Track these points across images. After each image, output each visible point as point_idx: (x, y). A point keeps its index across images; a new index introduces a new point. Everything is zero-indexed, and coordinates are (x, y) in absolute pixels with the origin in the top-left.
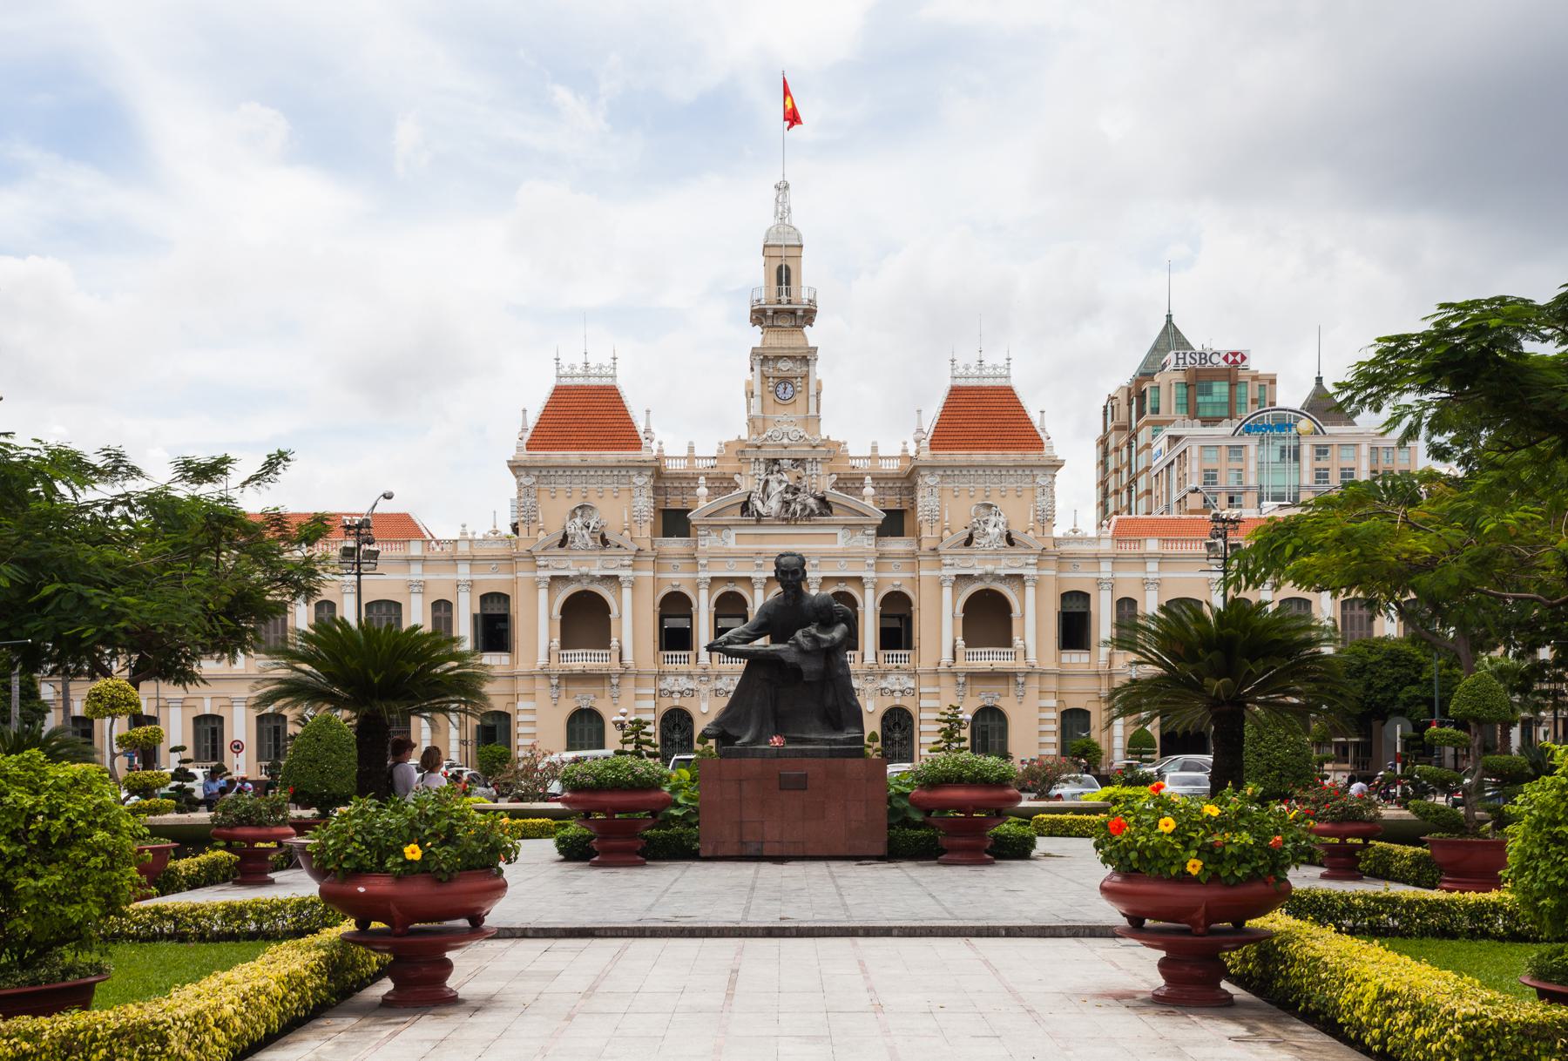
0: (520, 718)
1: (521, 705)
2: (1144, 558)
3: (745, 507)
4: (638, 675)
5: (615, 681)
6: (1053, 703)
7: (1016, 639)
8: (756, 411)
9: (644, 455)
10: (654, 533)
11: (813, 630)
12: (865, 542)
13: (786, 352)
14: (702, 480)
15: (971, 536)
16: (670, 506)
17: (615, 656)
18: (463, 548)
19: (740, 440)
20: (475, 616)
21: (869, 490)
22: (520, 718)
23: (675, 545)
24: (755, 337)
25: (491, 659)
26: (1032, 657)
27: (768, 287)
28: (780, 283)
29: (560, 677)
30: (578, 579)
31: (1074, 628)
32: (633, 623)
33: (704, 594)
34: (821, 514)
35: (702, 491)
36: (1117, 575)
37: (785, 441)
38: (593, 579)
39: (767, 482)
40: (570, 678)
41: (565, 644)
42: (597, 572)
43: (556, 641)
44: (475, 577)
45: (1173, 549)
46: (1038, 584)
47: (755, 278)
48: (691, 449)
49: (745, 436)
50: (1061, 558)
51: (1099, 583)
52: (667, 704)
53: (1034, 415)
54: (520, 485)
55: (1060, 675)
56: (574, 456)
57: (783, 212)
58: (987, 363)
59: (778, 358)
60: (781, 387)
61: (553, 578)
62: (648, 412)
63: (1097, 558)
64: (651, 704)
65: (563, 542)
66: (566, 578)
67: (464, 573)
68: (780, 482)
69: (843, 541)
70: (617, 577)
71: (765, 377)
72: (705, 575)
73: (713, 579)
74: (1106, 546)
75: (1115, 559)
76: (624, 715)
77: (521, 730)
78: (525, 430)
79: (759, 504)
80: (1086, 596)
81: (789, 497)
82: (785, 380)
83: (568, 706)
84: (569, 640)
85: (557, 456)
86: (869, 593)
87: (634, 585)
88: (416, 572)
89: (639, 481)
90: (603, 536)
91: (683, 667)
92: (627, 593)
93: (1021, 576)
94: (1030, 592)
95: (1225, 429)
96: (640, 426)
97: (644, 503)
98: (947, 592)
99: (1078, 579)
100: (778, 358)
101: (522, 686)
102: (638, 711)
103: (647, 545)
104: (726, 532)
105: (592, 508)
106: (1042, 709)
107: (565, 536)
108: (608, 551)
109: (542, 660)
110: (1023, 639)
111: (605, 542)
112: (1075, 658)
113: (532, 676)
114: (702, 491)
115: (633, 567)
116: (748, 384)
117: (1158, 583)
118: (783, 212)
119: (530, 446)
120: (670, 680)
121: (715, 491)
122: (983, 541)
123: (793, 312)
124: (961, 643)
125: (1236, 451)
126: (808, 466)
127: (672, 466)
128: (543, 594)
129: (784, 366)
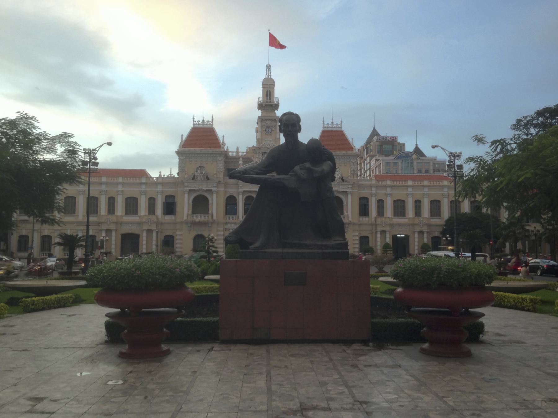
0: (177, 237)
1: (178, 233)
2: (386, 187)
5: (210, 225)
6: (357, 234)
7: (345, 212)
8: (259, 136)
9: (222, 150)
11: (308, 165)
13: (269, 118)
14: (241, 159)
16: (230, 168)
17: (210, 217)
18: (160, 180)
19: (253, 147)
20: (164, 203)
22: (177, 237)
24: (259, 113)
25: (169, 218)
26: (350, 219)
27: (263, 97)
29: (191, 223)
30: (199, 190)
31: (364, 210)
33: (241, 196)
35: (241, 162)
36: (378, 192)
38: (203, 191)
40: (195, 224)
42: (205, 188)
43: (190, 211)
44: (164, 190)
45: (396, 183)
46: (352, 194)
47: (258, 94)
48: (238, 149)
49: (255, 145)
50: (359, 186)
51: (371, 194)
53: (350, 140)
54: (180, 159)
55: (360, 225)
56: (198, 150)
57: (268, 72)
58: (335, 123)
59: (267, 120)
61: (190, 190)
62: (223, 136)
63: (371, 186)
64: (222, 233)
65: (193, 179)
66: (194, 190)
67: (160, 188)
70: (211, 190)
71: (262, 126)
72: (241, 190)
73: (244, 191)
74: (374, 182)
75: (377, 187)
77: (177, 241)
78: (182, 141)
80: (366, 199)
82: (268, 127)
83: (194, 234)
84: (194, 212)
85: (192, 150)
87: (217, 193)
88: (143, 188)
89: (220, 158)
90: (207, 177)
91: (233, 221)
92: (215, 196)
93: (346, 192)
94: (350, 197)
95: (391, 158)
96: (221, 140)
97: (221, 166)
99: (365, 193)
100: (267, 120)
102: (218, 235)
106: (354, 236)
108: (209, 181)
109: (185, 218)
110: (347, 212)
111: (208, 179)
112: (364, 219)
113: (181, 223)
114: (241, 162)
115: (217, 187)
116: (257, 128)
117: (391, 195)
118: (268, 72)
120: (229, 225)
121: (245, 163)
123: (271, 105)
125: (395, 164)
127: (231, 154)
128: (186, 196)
129: (268, 122)
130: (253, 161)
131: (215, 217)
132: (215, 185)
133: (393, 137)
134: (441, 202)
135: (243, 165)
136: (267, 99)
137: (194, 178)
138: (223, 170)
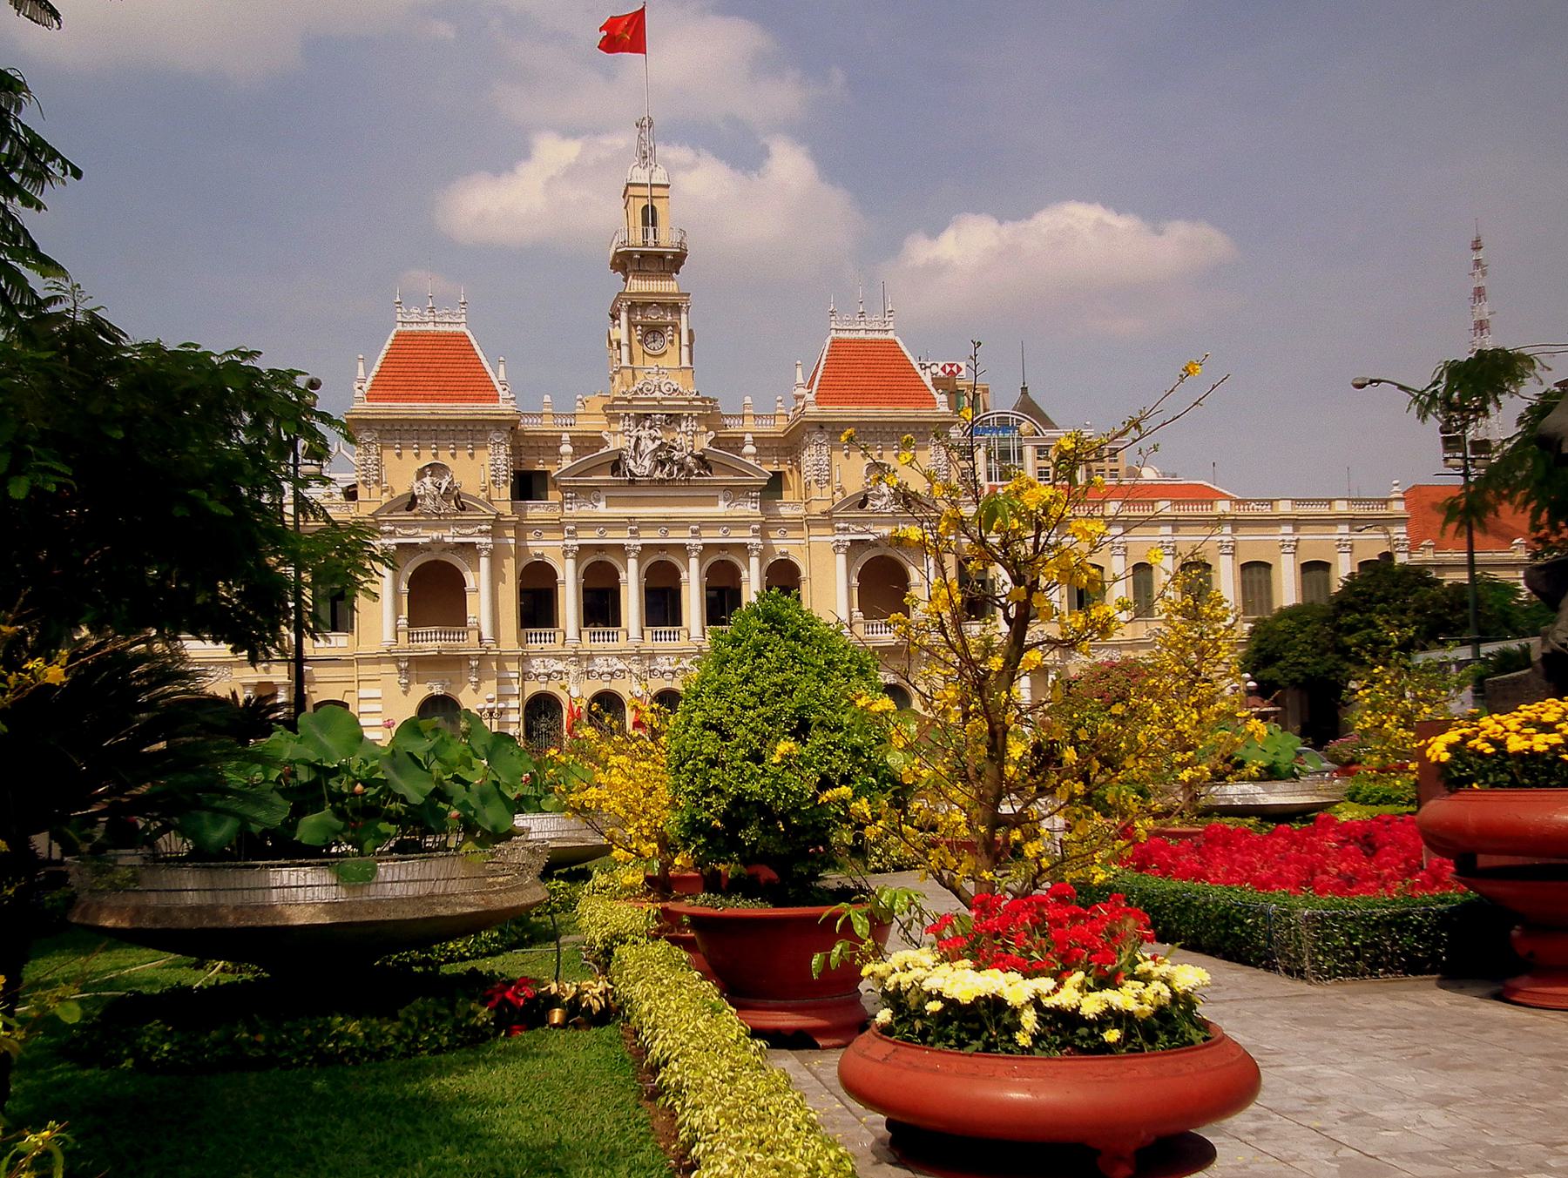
0: (364, 707)
3: (616, 465)
4: (501, 659)
9: (505, 406)
10: (514, 498)
12: (749, 509)
15: (866, 497)
17: (474, 635)
21: (750, 449)
23: (536, 511)
28: (645, 223)
30: (425, 548)
32: (489, 599)
33: (570, 564)
34: (699, 474)
35: (566, 448)
37: (657, 394)
39: (638, 439)
41: (412, 622)
43: (403, 621)
52: (533, 688)
60: (650, 338)
68: (654, 439)
69: (721, 509)
71: (632, 324)
76: (491, 701)
79: (631, 463)
81: (663, 454)
83: (421, 692)
86: (754, 562)
92: (484, 563)
98: (841, 559)
101: (367, 670)
103: (506, 508)
104: (595, 494)
105: (444, 467)
107: (414, 498)
114: (566, 448)
119: (372, 396)
122: (878, 503)
123: (661, 256)
124: (858, 615)
126: (684, 424)
129: (653, 316)
130: (602, 442)
131: (486, 634)
132: (484, 527)
133: (951, 366)
134: (1273, 571)
135: (574, 456)
136: (645, 234)
137: (412, 502)
138: (505, 473)
